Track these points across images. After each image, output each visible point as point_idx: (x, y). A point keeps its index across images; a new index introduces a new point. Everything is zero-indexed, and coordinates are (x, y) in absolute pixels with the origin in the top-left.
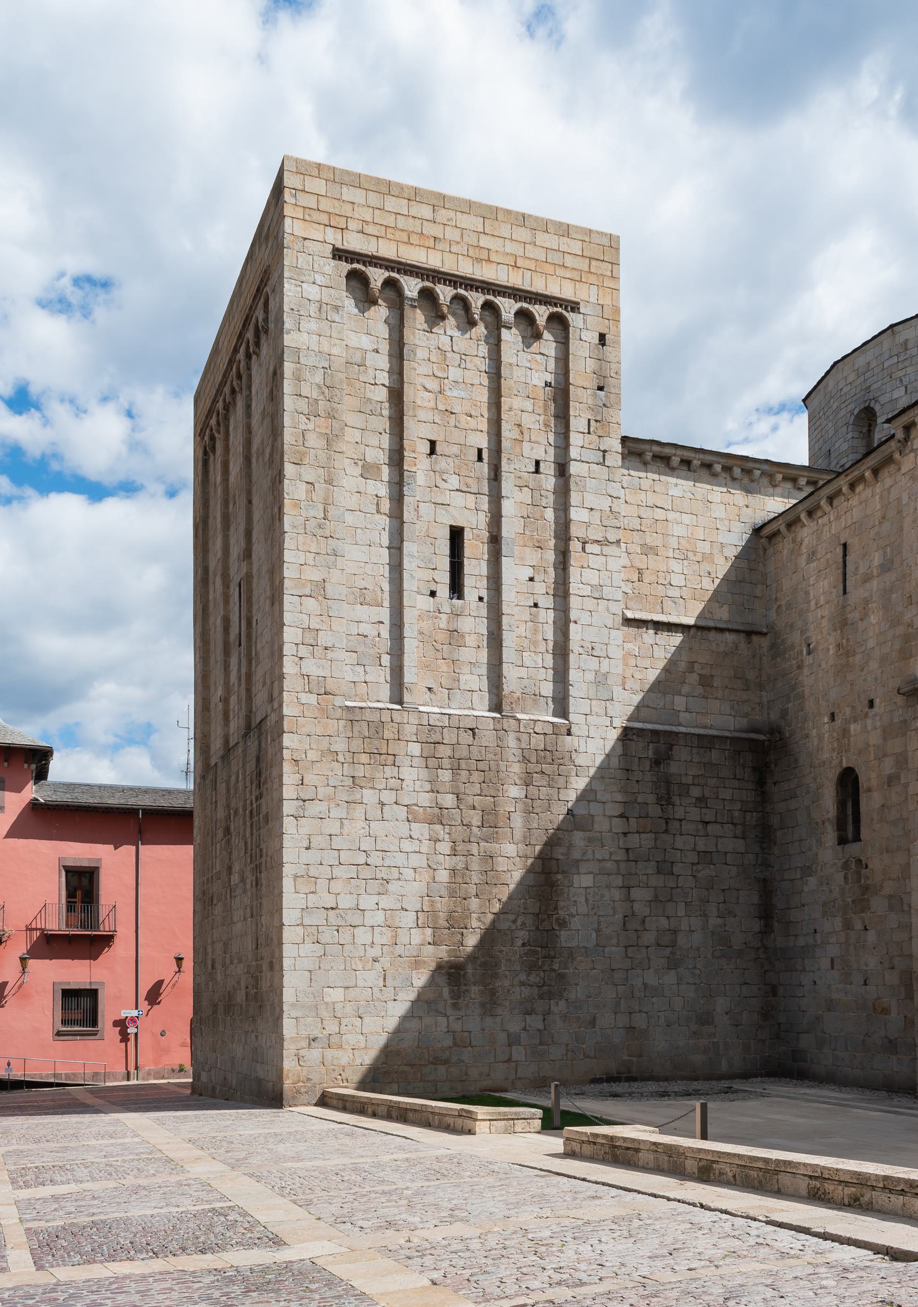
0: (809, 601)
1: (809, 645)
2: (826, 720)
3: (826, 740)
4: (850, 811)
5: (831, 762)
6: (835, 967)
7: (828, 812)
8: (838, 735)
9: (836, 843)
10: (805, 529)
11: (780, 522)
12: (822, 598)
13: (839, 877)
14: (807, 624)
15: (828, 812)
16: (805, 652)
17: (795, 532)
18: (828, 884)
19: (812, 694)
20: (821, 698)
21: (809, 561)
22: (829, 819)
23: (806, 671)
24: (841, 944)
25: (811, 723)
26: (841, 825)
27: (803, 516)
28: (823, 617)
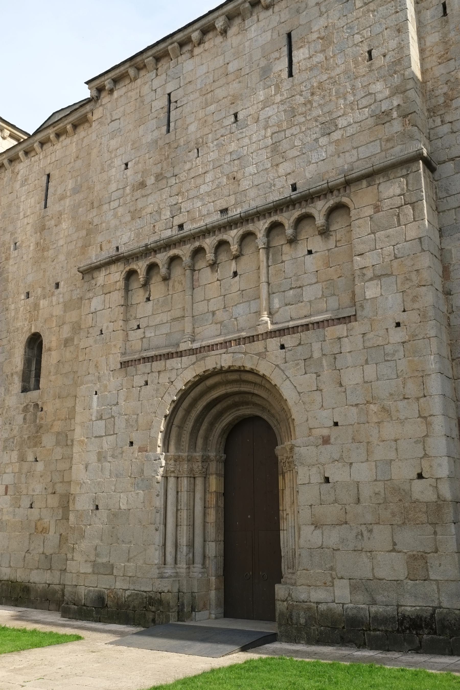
0: (19, 213)
1: (16, 244)
2: (23, 297)
3: (21, 312)
4: (33, 368)
5: (22, 329)
6: (8, 493)
7: (17, 367)
8: (30, 308)
9: (20, 391)
10: (22, 164)
11: (4, 157)
12: (29, 210)
13: (19, 419)
14: (16, 228)
15: (17, 367)
16: (12, 248)
17: (14, 166)
18: (10, 423)
19: (14, 278)
20: (20, 281)
21: (22, 185)
22: (16, 372)
23: (11, 262)
24: (15, 473)
25: (11, 299)
26: (25, 378)
27: (21, 154)
28: (28, 224)
